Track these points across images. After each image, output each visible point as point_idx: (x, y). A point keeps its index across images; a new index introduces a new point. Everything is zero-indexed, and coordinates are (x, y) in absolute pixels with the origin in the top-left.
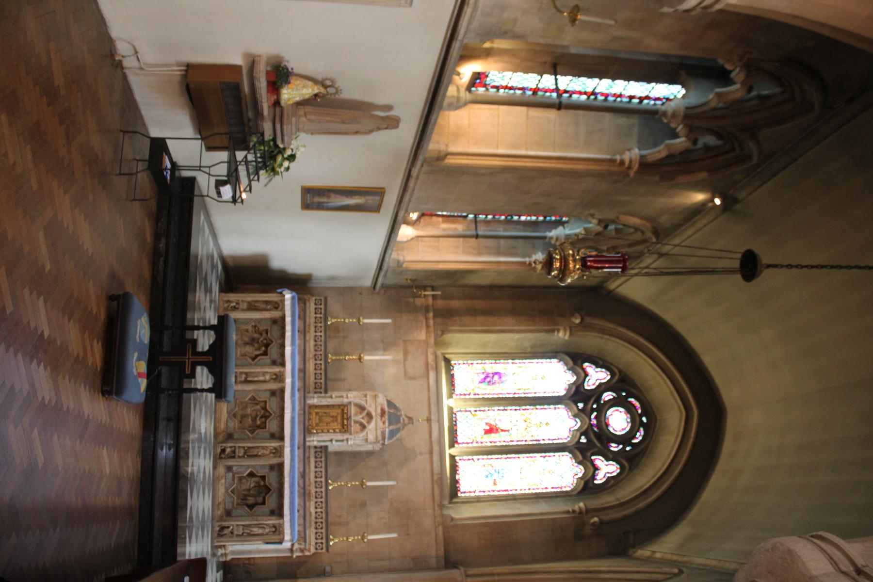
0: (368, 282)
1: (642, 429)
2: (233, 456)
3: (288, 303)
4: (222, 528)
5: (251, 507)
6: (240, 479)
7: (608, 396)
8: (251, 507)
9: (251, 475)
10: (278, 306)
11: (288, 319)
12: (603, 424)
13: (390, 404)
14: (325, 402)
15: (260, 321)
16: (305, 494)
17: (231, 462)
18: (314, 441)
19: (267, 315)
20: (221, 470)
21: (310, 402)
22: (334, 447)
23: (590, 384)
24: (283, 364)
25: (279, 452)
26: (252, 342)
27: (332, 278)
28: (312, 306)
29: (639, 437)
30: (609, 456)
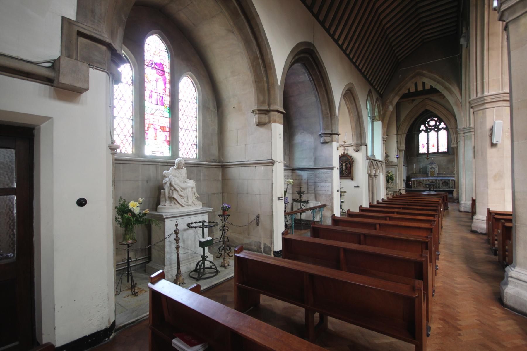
0: (406, 167)
1: (434, 119)
2: (439, 186)
3: (414, 179)
4: (451, 188)
5: (448, 184)
6: (443, 185)
7: (427, 125)
8: (448, 184)
9: (442, 184)
10: (414, 181)
11: (416, 179)
12: (433, 126)
13: (430, 164)
14: (429, 174)
15: (416, 183)
16: (446, 176)
17: (440, 187)
18: (436, 175)
19: (415, 182)
20: (442, 188)
21: (429, 176)
22: (437, 172)
23: (425, 129)
24: (424, 180)
25: (439, 180)
26: (420, 184)
27: (406, 173)
28: (412, 176)
29: (436, 119)
30: (440, 124)
